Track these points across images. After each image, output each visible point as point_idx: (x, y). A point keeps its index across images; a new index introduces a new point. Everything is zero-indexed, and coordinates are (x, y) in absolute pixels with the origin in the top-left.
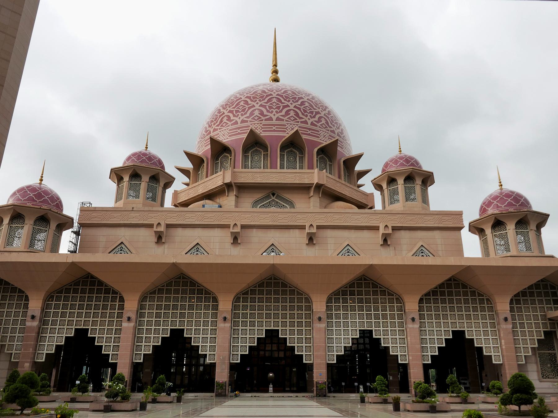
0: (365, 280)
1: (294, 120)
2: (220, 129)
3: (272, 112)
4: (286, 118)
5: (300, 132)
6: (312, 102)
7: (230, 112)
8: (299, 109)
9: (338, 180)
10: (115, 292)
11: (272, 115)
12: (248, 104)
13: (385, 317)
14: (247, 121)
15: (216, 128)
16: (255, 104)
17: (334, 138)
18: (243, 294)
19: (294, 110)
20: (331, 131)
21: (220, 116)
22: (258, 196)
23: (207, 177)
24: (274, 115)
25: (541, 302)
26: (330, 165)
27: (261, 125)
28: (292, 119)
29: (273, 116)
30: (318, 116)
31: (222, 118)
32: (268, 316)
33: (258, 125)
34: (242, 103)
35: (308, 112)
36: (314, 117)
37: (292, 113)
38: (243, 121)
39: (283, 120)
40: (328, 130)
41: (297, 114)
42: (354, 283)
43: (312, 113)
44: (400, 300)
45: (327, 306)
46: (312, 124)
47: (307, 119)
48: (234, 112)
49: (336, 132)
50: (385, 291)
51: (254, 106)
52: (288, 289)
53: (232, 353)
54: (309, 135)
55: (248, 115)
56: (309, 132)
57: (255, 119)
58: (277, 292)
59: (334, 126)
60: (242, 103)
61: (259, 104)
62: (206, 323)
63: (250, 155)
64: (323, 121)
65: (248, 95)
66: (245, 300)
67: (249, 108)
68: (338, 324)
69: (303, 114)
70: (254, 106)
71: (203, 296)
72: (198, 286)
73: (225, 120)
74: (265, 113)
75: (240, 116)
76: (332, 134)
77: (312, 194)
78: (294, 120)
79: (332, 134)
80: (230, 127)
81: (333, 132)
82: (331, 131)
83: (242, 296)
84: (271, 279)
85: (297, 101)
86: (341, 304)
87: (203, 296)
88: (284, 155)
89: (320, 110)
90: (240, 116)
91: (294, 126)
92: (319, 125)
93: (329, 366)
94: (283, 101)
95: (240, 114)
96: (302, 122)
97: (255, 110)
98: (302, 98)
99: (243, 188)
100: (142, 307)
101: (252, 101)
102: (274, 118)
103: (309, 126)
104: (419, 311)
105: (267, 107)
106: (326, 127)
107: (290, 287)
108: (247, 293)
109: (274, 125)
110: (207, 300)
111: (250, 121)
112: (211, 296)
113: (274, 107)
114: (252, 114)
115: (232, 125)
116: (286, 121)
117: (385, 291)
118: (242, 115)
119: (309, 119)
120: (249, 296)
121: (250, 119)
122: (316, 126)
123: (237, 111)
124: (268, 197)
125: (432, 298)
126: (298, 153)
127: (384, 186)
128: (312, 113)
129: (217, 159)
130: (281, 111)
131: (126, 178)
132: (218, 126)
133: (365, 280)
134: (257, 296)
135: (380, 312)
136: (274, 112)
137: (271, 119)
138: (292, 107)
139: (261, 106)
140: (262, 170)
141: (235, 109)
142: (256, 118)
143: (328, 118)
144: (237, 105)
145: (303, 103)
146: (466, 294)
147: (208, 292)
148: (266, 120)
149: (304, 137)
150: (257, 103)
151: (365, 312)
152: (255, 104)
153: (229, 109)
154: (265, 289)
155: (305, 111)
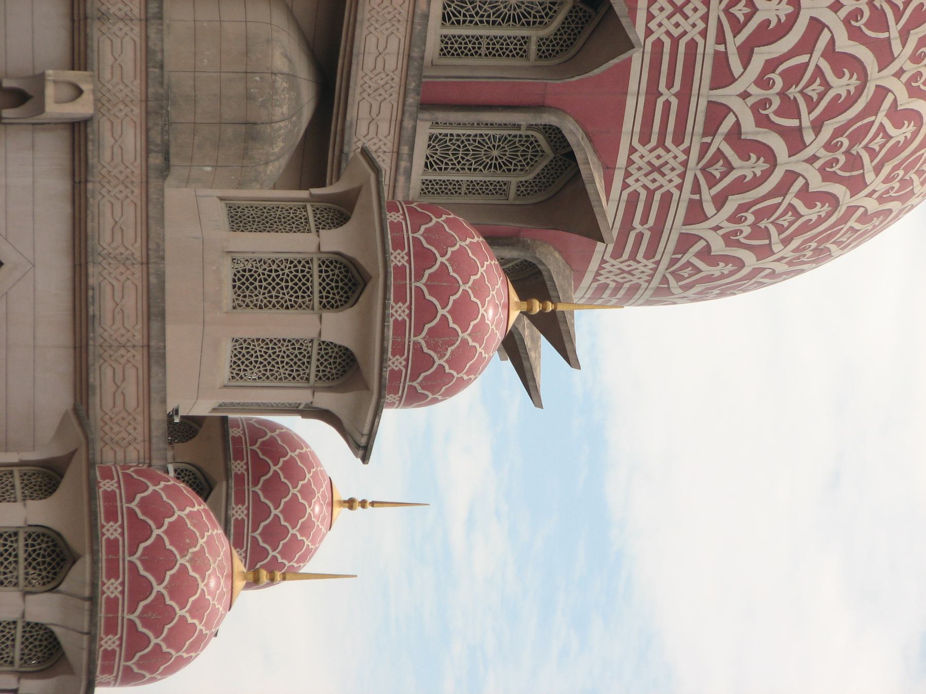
1: (732, 18)
6: (873, 108)
8: (806, 45)
19: (793, 19)
35: (793, 92)
40: (696, 189)
43: (789, 108)
59: (735, 218)
64: (747, 168)
69: (771, 65)
78: (732, 18)
85: (855, 34)
89: (815, 145)
92: (719, 142)
96: (721, 60)
103: (703, 95)
119: (745, 95)
122: (711, 129)
143: (782, 189)
145: (841, 62)
155: (793, 76)
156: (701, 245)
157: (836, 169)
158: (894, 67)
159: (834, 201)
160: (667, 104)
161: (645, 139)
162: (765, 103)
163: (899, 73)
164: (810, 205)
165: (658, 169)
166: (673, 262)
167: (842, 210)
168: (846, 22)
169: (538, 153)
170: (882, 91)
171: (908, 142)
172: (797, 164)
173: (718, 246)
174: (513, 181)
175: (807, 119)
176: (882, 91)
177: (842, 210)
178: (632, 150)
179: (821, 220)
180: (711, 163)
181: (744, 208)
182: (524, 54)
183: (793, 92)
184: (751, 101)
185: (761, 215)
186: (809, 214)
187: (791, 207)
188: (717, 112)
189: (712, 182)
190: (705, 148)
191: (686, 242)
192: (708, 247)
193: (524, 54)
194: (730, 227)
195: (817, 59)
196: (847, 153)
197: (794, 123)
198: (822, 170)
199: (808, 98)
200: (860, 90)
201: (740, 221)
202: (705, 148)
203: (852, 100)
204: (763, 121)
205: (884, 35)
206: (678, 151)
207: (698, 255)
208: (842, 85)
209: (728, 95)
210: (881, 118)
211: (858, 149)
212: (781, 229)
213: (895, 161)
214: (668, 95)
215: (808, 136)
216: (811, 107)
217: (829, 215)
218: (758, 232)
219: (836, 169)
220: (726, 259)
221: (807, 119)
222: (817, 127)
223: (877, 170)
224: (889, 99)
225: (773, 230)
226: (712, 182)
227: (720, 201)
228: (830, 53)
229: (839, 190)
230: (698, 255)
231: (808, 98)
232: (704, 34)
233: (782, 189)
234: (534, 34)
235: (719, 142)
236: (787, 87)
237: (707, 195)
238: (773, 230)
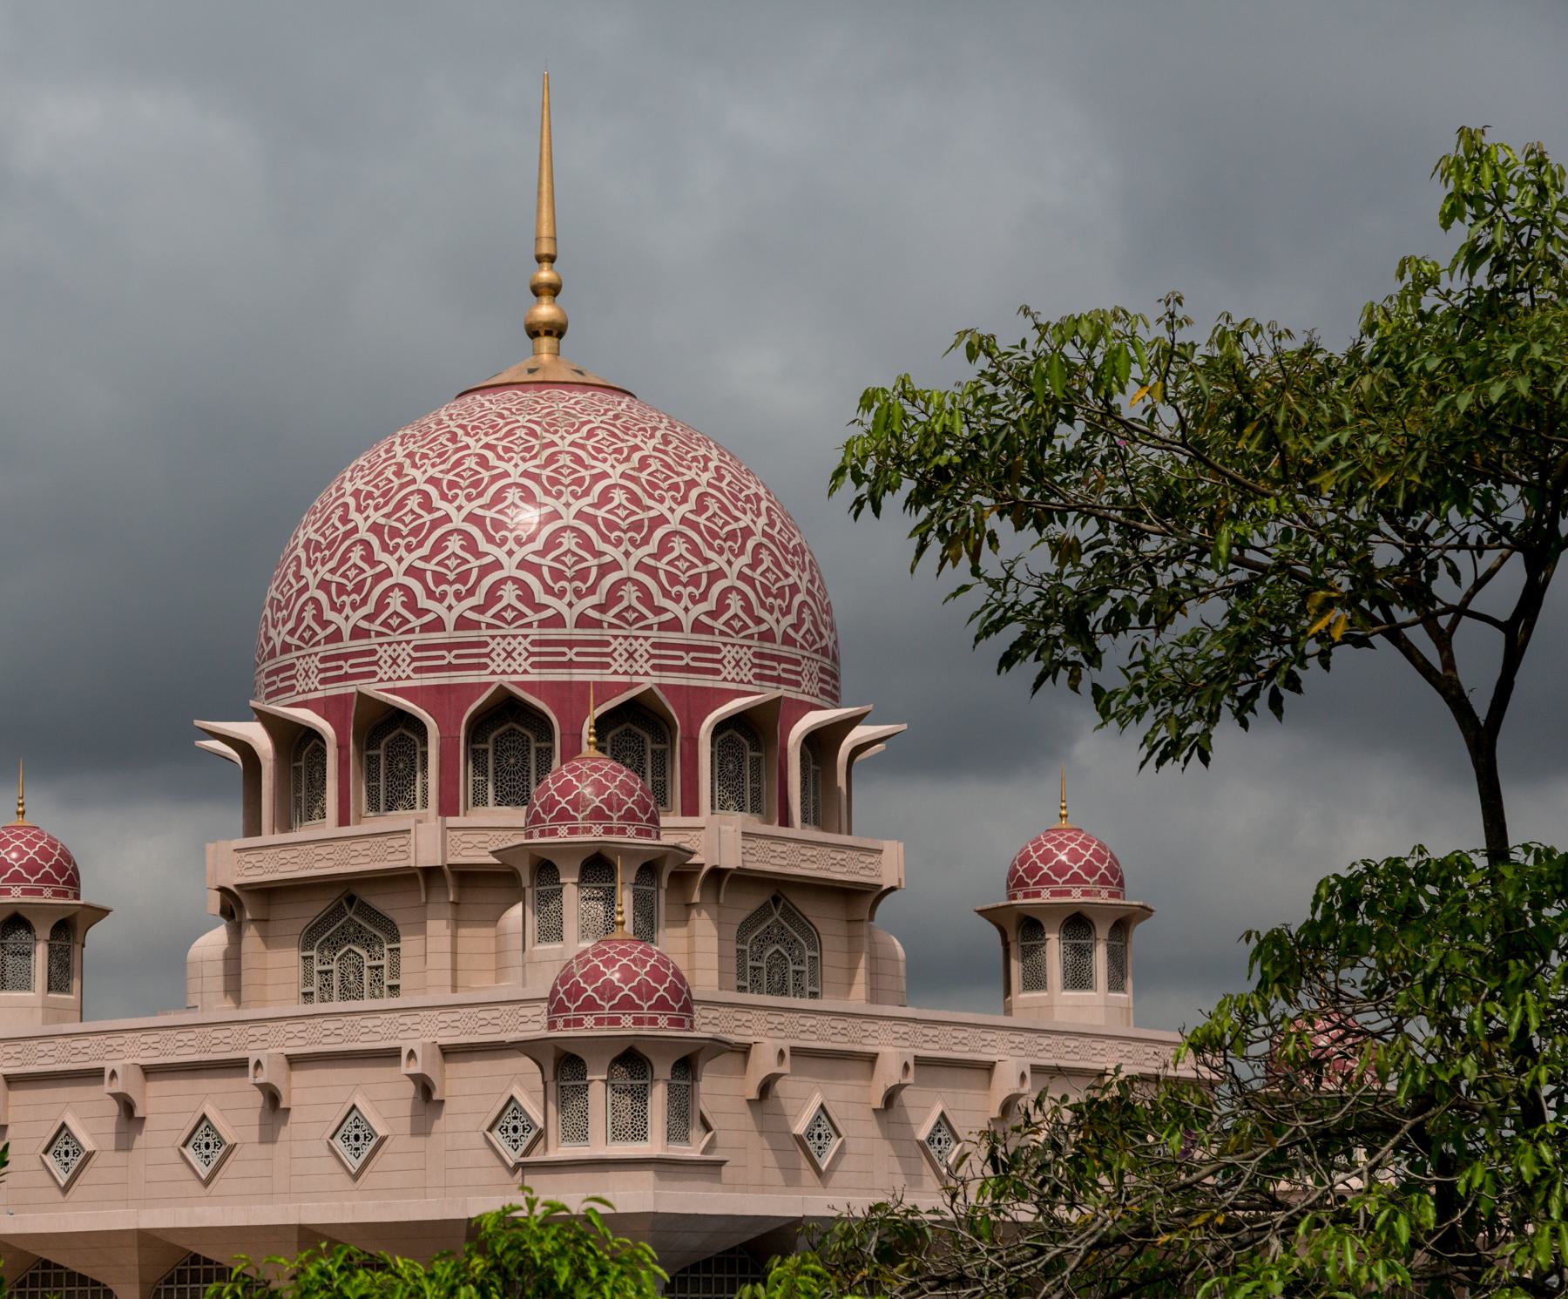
1: (637, 620)
4: (609, 617)
6: (695, 526)
8: (653, 572)
9: (775, 829)
11: (559, 605)
12: (479, 555)
14: (476, 625)
15: (364, 625)
19: (636, 582)
26: (756, 762)
28: (631, 616)
29: (566, 612)
33: (514, 643)
34: (454, 544)
35: (684, 579)
36: (704, 597)
37: (630, 595)
39: (598, 624)
40: (751, 637)
41: (646, 598)
47: (676, 609)
48: (429, 576)
51: (497, 565)
55: (478, 599)
57: (504, 620)
59: (771, 610)
60: (454, 544)
61: (517, 558)
65: (473, 507)
67: (485, 571)
69: (666, 594)
73: (396, 601)
74: (541, 597)
75: (450, 599)
77: (696, 898)
78: (637, 620)
80: (419, 638)
81: (767, 636)
85: (646, 541)
89: (719, 562)
90: (450, 599)
91: (636, 644)
92: (718, 624)
94: (600, 545)
95: (450, 590)
96: (663, 626)
97: (503, 581)
101: (490, 539)
102: (570, 616)
105: (545, 571)
109: (570, 644)
111: (489, 626)
113: (569, 573)
114: (492, 596)
115: (425, 628)
118: (459, 597)
119: (686, 609)
121: (486, 618)
122: (710, 630)
126: (648, 740)
128: (695, 581)
130: (592, 590)
132: (369, 618)
137: (557, 621)
138: (628, 569)
142: (509, 615)
144: (438, 547)
145: (664, 548)
148: (543, 624)
150: (510, 553)
156: (790, 631)
157: (736, 547)
158: (668, 514)
159: (759, 546)
160: (693, 659)
161: (717, 672)
162: (691, 596)
163: (672, 510)
164: (762, 561)
165: (737, 664)
166: (802, 647)
167: (765, 541)
168: (637, 547)
169: (730, 739)
170: (684, 520)
171: (719, 501)
172: (732, 573)
173: (791, 618)
174: (749, 754)
175: (702, 569)
176: (684, 520)
177: (765, 541)
178: (725, 679)
179: (772, 554)
180: (732, 628)
181: (763, 605)
182: (663, 752)
183: (684, 579)
184: (690, 605)
185: (768, 593)
186: (767, 562)
187: (762, 574)
188: (698, 627)
189: (745, 627)
190: (722, 633)
191: (788, 640)
192: (792, 626)
193: (663, 752)
194: (777, 614)
195: (662, 564)
196: (725, 540)
197: (705, 576)
198: (737, 556)
199: (689, 569)
200: (682, 535)
201: (772, 607)
202: (722, 633)
203: (689, 540)
205: (646, 523)
206: (725, 651)
207: (797, 631)
208: (679, 546)
209: (687, 622)
210: (702, 520)
211: (723, 533)
212: (778, 579)
213: (731, 508)
215: (713, 567)
216: (694, 566)
217: (768, 548)
218: (780, 594)
219: (736, 547)
220: (800, 612)
221: (702, 569)
222: (707, 561)
223: (737, 519)
224: (689, 516)
225: (779, 584)
226: (745, 627)
227: (759, 621)
228: (657, 556)
229: (750, 544)
230: (797, 631)
231: (689, 569)
232: (646, 638)
233: (750, 581)
234: (649, 746)
235: (718, 624)
236: (681, 583)
237: (754, 629)
238: (779, 584)
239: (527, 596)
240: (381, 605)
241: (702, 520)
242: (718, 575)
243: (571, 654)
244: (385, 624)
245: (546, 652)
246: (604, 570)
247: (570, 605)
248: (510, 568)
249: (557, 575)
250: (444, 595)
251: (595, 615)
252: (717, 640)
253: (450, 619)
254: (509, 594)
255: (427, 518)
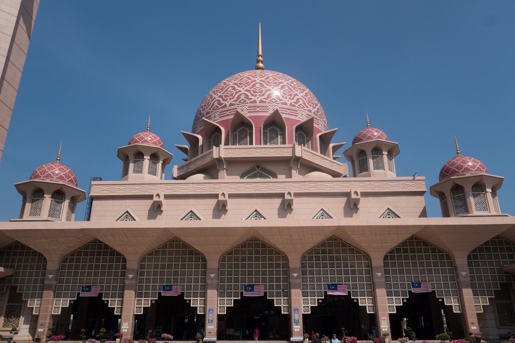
0: (335, 239)
2: (212, 112)
3: (256, 96)
4: (268, 101)
5: (280, 112)
6: (291, 85)
7: (220, 97)
10: (119, 254)
11: (256, 98)
13: (353, 272)
14: (234, 105)
15: (209, 111)
16: (241, 89)
17: (311, 116)
18: (228, 254)
20: (308, 111)
21: (212, 101)
22: (245, 168)
23: (202, 152)
24: (258, 98)
25: (497, 257)
27: (246, 107)
30: (296, 98)
31: (214, 103)
32: (250, 273)
38: (231, 105)
39: (265, 102)
40: (305, 110)
42: (325, 243)
43: (291, 95)
44: (367, 257)
45: (302, 264)
46: (291, 105)
47: (286, 100)
48: (224, 97)
49: (313, 111)
50: (353, 249)
51: (240, 91)
52: (267, 249)
53: (219, 305)
54: (288, 114)
55: (235, 99)
56: (289, 112)
58: (257, 252)
59: (311, 106)
60: (230, 89)
62: (196, 280)
63: (237, 133)
64: (301, 102)
65: (236, 82)
66: (230, 260)
67: (237, 93)
68: (312, 280)
70: (240, 91)
71: (194, 256)
72: (189, 248)
73: (216, 104)
74: (250, 97)
76: (310, 113)
79: (310, 113)
81: (310, 111)
82: (308, 111)
83: (227, 256)
84: (252, 240)
86: (314, 262)
87: (194, 256)
88: (267, 132)
89: (298, 93)
92: (297, 105)
93: (136, 317)
96: (282, 104)
97: (241, 94)
98: (282, 83)
99: (232, 163)
100: (142, 267)
101: (239, 87)
102: (258, 101)
103: (288, 106)
104: (384, 266)
106: (303, 107)
107: (269, 247)
108: (231, 253)
109: (258, 107)
110: (197, 260)
111: (237, 104)
112: (200, 256)
113: (258, 91)
114: (238, 98)
116: (268, 103)
117: (353, 249)
118: (230, 99)
119: (288, 101)
120: (234, 256)
121: (237, 103)
122: (295, 106)
123: (226, 96)
124: (253, 170)
125: (396, 254)
126: (279, 130)
127: (355, 157)
128: (291, 95)
129: (210, 138)
130: (263, 95)
131: (131, 157)
132: (210, 109)
133: (335, 239)
134: (240, 256)
135: (349, 269)
136: (258, 96)
137: (255, 102)
139: (246, 90)
140: (249, 146)
141: (225, 94)
142: (242, 101)
146: (426, 251)
147: (198, 253)
148: (251, 102)
149: (283, 116)
150: (243, 88)
151: (335, 269)
152: (241, 89)
153: (219, 94)
154: (247, 249)
162: (289, 98)
169: (301, 134)
185: (310, 102)
204: (293, 99)
209: (289, 103)
214: (289, 112)
227: (307, 107)
237: (306, 108)
239: (247, 96)
240: (213, 105)
241: (292, 85)
242: (296, 95)
243: (258, 109)
244: (213, 109)
245: (251, 109)
246: (267, 91)
247: (258, 98)
248: (243, 91)
249: (254, 92)
250: (227, 99)
251: (264, 100)
252: (296, 109)
253: (228, 104)
254: (242, 97)
255: (224, 86)
